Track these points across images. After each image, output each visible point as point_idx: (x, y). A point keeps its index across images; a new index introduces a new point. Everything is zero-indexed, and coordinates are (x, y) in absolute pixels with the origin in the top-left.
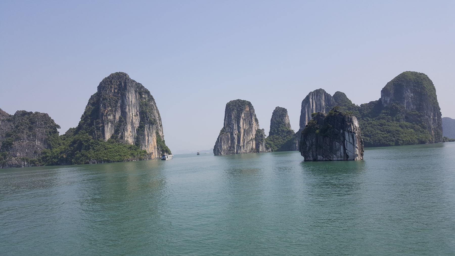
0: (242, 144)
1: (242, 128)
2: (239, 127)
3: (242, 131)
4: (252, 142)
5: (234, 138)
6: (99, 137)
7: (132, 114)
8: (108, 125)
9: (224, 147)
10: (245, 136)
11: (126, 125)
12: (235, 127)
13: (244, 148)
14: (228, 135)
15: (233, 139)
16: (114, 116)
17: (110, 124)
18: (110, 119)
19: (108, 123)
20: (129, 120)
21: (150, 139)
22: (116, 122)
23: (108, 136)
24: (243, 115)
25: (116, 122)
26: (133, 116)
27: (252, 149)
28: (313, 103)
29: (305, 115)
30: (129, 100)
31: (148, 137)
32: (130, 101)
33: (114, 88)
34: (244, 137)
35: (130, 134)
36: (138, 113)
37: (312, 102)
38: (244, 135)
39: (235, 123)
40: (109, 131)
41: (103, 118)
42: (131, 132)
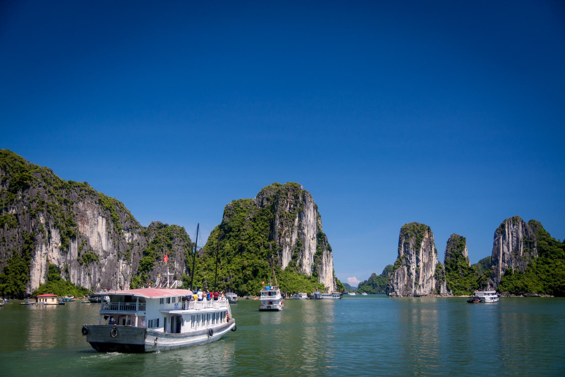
0: (421, 283)
1: (421, 261)
2: (418, 260)
3: (421, 264)
4: (431, 281)
5: (411, 274)
6: (277, 262)
7: (310, 237)
8: (286, 249)
9: (400, 286)
10: (425, 272)
11: (304, 250)
12: (414, 259)
13: (423, 288)
14: (404, 270)
15: (410, 274)
16: (291, 238)
17: (288, 248)
18: (287, 241)
19: (286, 247)
20: (307, 245)
21: (327, 270)
22: (292, 245)
23: (285, 263)
24: (423, 244)
25: (292, 245)
26: (311, 240)
27: (432, 290)
28: (509, 234)
29: (500, 249)
30: (308, 219)
31: (326, 266)
32: (309, 220)
33: (290, 204)
34: (424, 274)
35: (307, 262)
36: (315, 235)
37: (508, 232)
38: (424, 270)
39: (414, 253)
40: (286, 256)
41: (281, 240)
42: (308, 259)
